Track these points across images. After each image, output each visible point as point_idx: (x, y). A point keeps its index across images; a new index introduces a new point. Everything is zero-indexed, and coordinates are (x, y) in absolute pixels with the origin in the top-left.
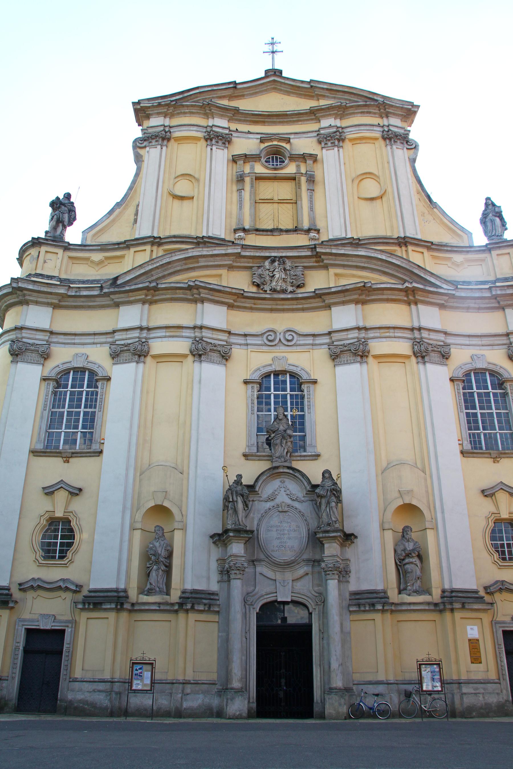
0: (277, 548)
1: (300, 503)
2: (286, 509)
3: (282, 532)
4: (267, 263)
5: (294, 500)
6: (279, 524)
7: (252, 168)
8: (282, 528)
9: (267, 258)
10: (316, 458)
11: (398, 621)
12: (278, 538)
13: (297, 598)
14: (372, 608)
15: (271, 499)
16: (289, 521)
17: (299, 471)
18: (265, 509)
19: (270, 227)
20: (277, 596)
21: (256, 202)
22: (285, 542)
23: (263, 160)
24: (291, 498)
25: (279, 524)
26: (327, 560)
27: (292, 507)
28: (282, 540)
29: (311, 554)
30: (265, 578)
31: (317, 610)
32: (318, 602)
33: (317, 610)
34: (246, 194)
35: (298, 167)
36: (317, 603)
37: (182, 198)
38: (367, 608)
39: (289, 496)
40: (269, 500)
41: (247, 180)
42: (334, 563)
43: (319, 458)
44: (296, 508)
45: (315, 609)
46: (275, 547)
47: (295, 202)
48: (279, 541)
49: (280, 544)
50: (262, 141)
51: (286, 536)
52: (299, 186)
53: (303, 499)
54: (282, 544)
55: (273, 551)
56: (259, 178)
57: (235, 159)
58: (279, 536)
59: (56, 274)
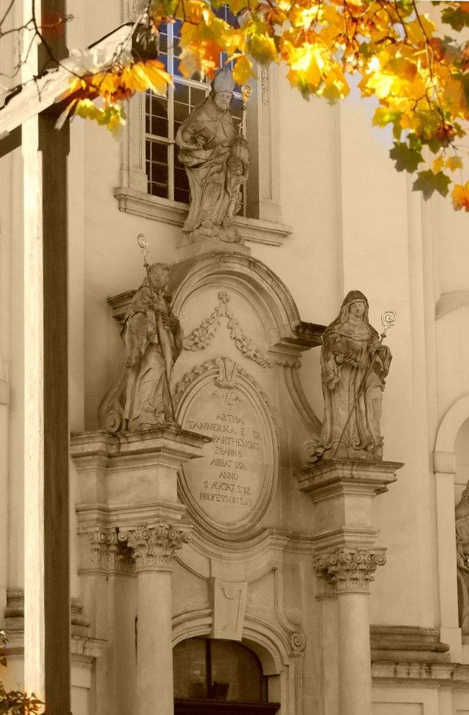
0: (215, 492)
1: (261, 368)
2: (234, 380)
3: (225, 447)
5: (249, 357)
6: (219, 422)
8: (226, 434)
10: (280, 240)
11: (457, 711)
12: (219, 463)
13: (254, 634)
14: (425, 676)
15: (200, 345)
16: (240, 415)
17: (270, 274)
18: (184, 371)
20: (211, 625)
22: (233, 476)
24: (245, 350)
25: (219, 422)
26: (350, 542)
27: (247, 376)
28: (226, 469)
29: (281, 516)
30: (184, 571)
31: (292, 669)
32: (295, 648)
33: (292, 669)
36: (293, 649)
38: (414, 675)
39: (239, 345)
40: (194, 348)
42: (373, 552)
43: (285, 241)
44: (254, 383)
45: (288, 666)
46: (210, 486)
48: (219, 470)
49: (222, 480)
51: (235, 459)
53: (267, 357)
54: (226, 481)
55: (204, 496)
58: (220, 457)
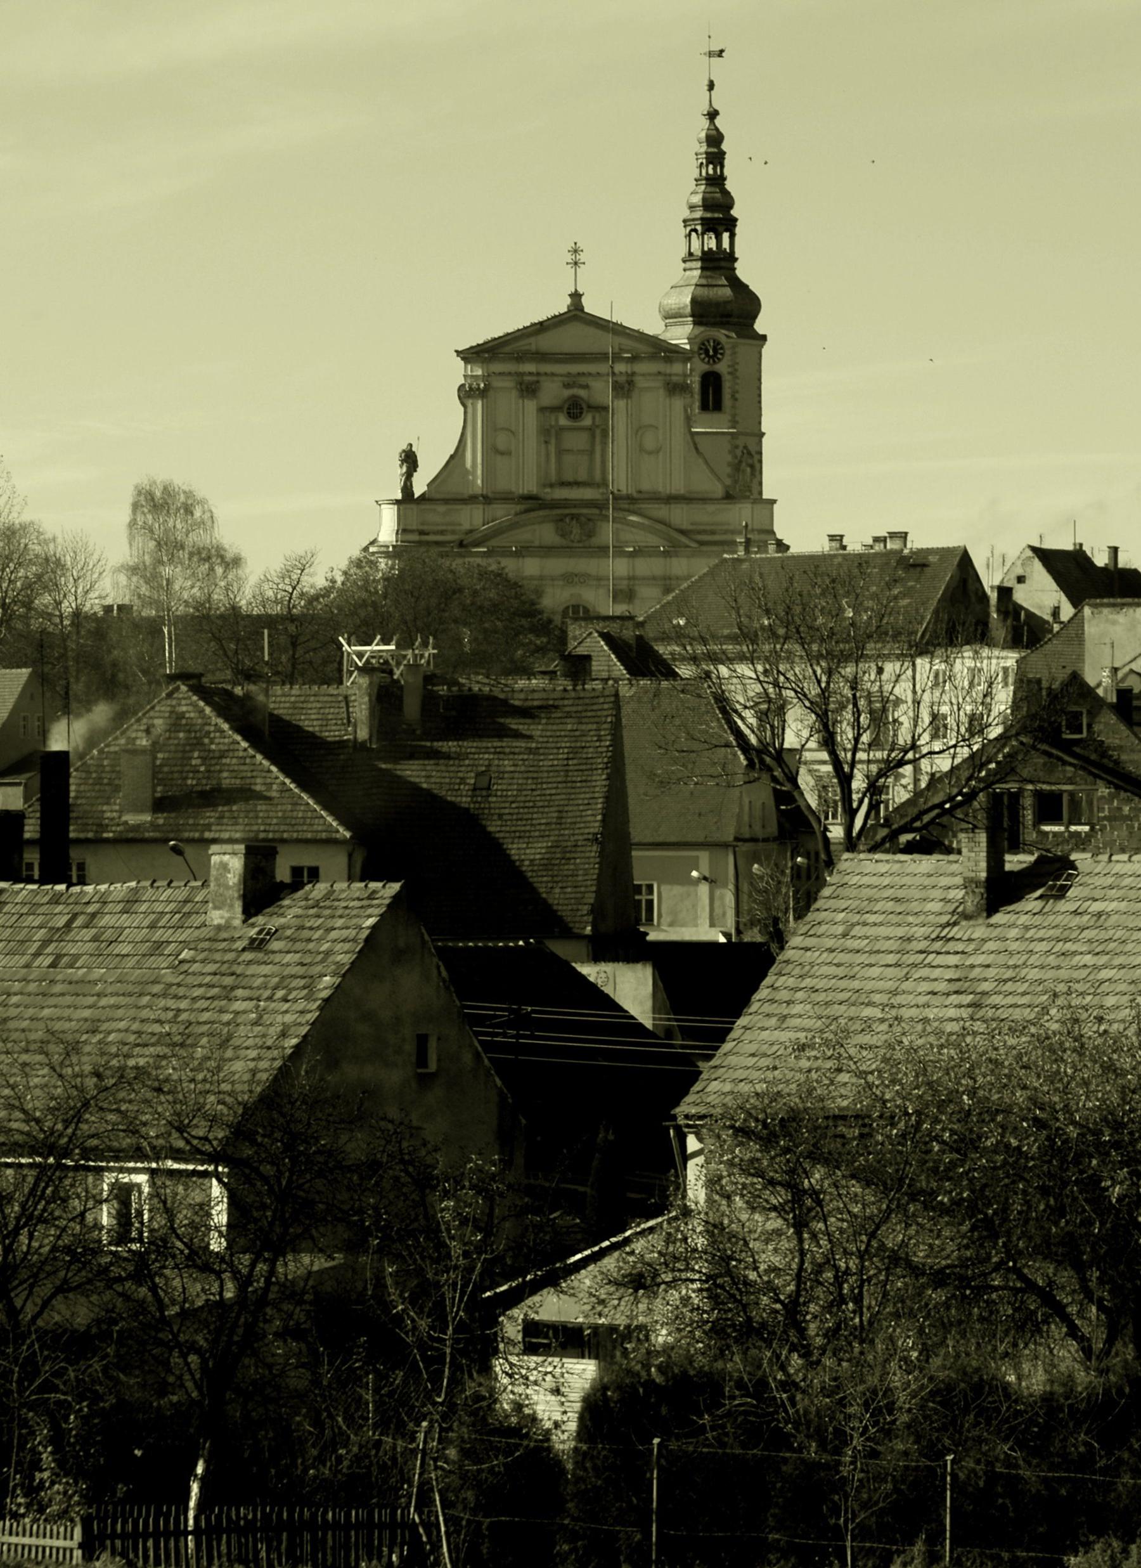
4: (567, 520)
7: (557, 420)
9: (567, 515)
19: (571, 479)
21: (560, 452)
23: (565, 411)
34: (552, 448)
35: (594, 418)
37: (502, 454)
41: (553, 432)
47: (591, 453)
50: (567, 386)
52: (593, 436)
56: (562, 429)
57: (542, 410)
59: (414, 527)
